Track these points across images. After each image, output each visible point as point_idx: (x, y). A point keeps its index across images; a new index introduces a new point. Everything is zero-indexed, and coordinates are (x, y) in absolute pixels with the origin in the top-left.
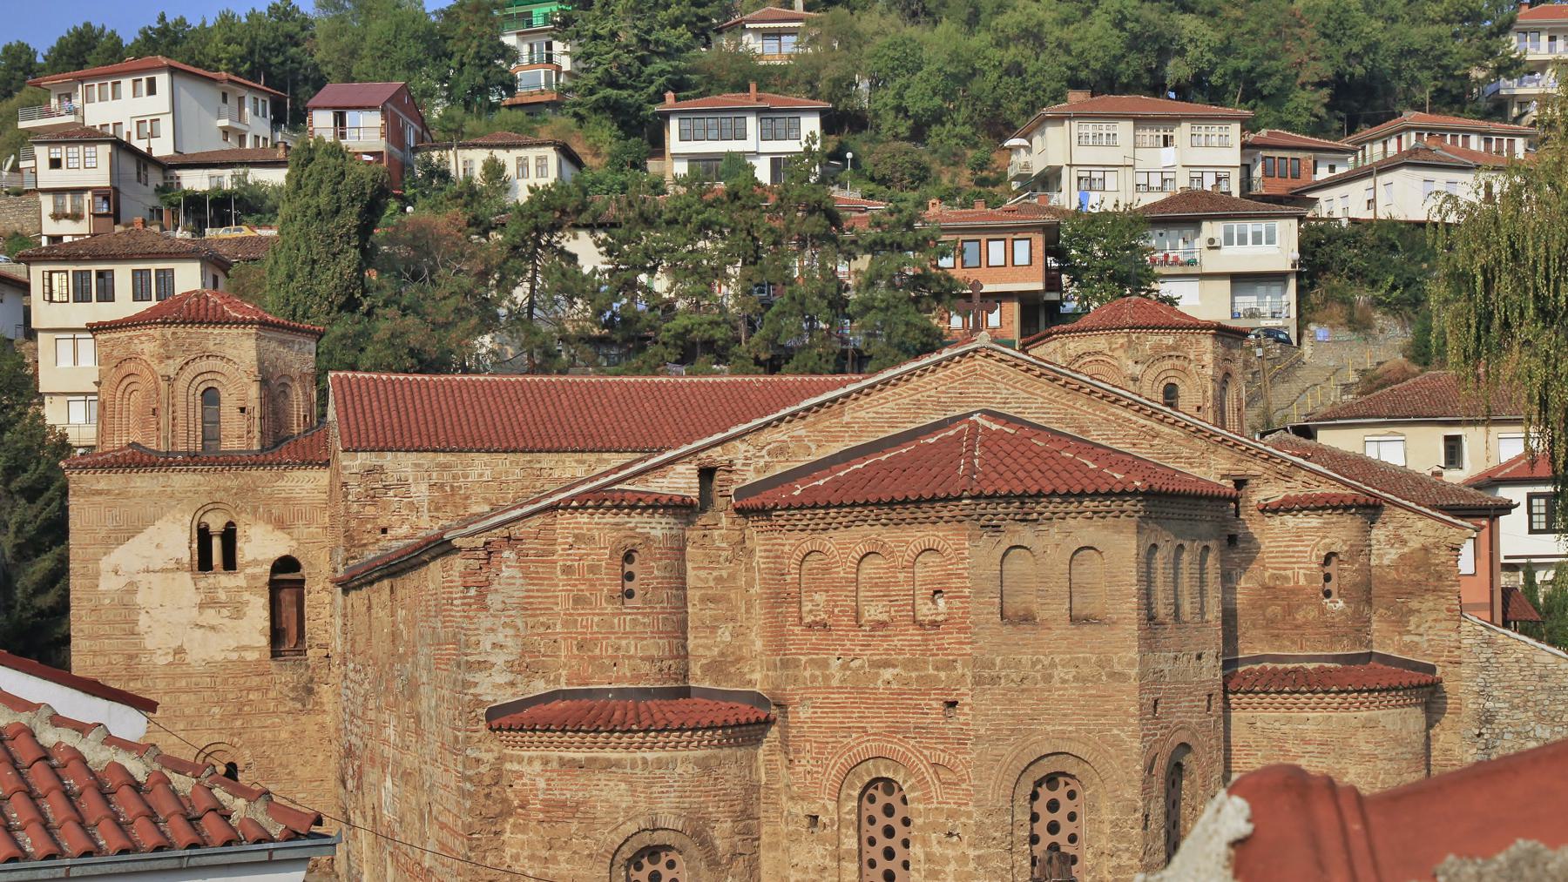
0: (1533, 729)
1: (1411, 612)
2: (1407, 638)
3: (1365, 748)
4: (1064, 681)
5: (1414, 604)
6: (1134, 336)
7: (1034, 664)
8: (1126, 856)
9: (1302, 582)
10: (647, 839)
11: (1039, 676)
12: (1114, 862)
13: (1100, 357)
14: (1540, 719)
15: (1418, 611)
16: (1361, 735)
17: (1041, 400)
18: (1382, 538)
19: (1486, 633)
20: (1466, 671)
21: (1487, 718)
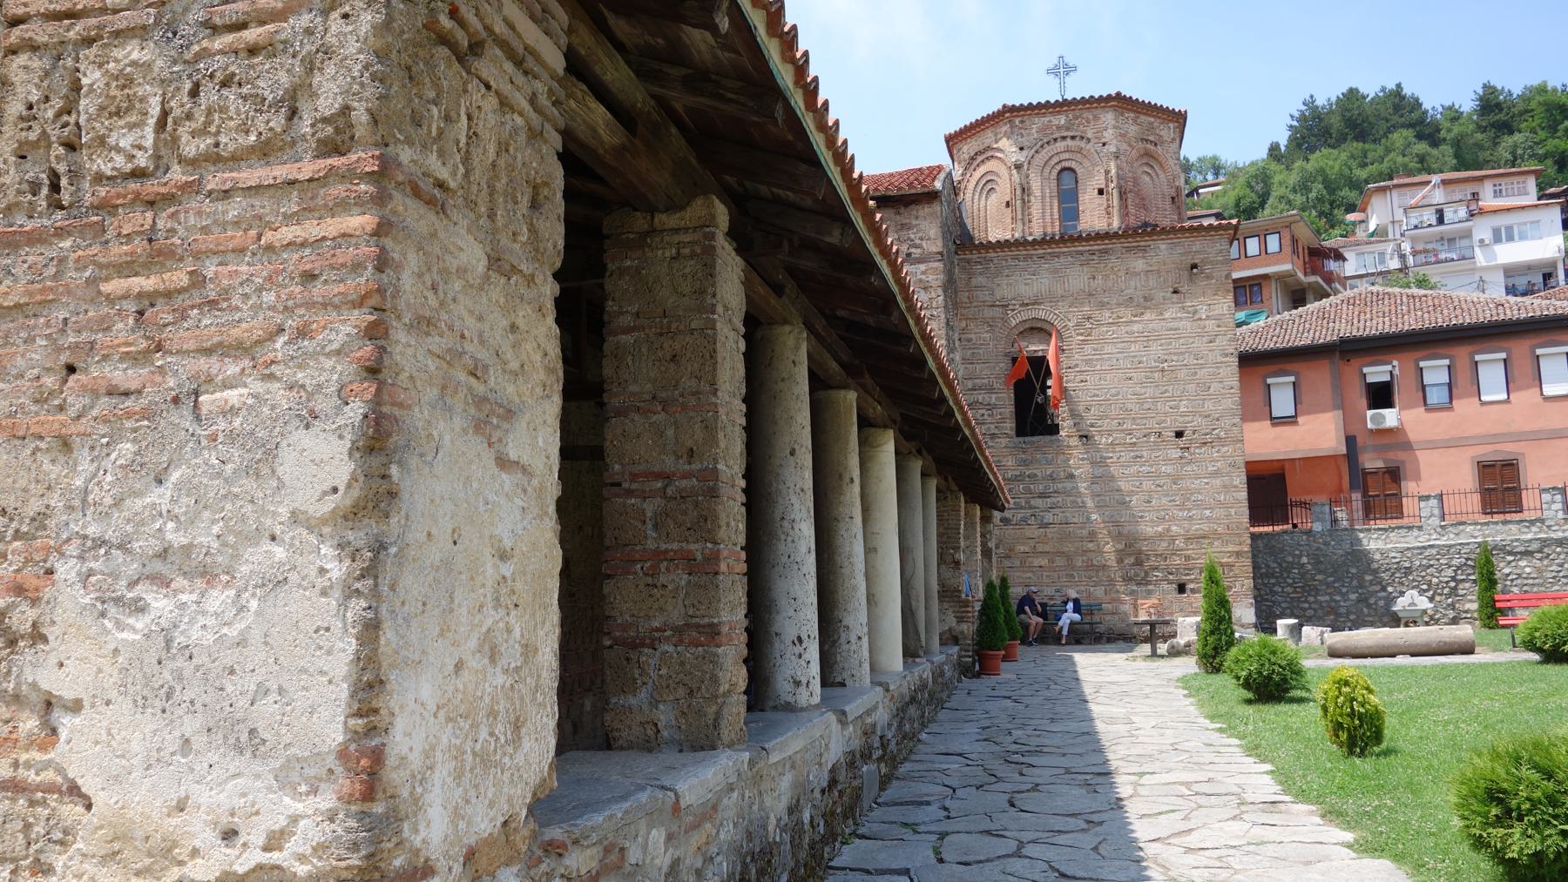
6: (1017, 121)
13: (990, 154)
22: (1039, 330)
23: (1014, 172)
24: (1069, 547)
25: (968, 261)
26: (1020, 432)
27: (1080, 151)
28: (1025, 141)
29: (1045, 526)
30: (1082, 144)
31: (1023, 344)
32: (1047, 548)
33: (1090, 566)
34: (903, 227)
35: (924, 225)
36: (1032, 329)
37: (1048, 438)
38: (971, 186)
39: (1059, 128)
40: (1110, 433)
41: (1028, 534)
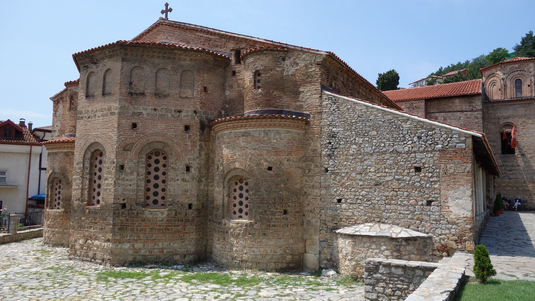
0: (355, 139)
1: (300, 93)
2: (298, 104)
3: (243, 144)
4: (99, 117)
5: (301, 89)
7: (92, 111)
8: (111, 179)
9: (249, 84)
10: (53, 176)
11: (93, 115)
12: (107, 182)
14: (358, 135)
15: (303, 92)
16: (241, 139)
17: (176, 35)
18: (288, 64)
19: (334, 98)
20: (324, 116)
21: (333, 136)
22: (510, 125)
23: (502, 81)
24: (518, 185)
25: (488, 107)
26: (503, 153)
27: (522, 74)
28: (505, 72)
29: (511, 179)
30: (523, 72)
31: (504, 129)
32: (511, 185)
33: (524, 190)
34: (471, 102)
35: (477, 102)
36: (507, 125)
37: (511, 155)
38: (488, 84)
39: (516, 68)
40: (531, 154)
41: (505, 181)
